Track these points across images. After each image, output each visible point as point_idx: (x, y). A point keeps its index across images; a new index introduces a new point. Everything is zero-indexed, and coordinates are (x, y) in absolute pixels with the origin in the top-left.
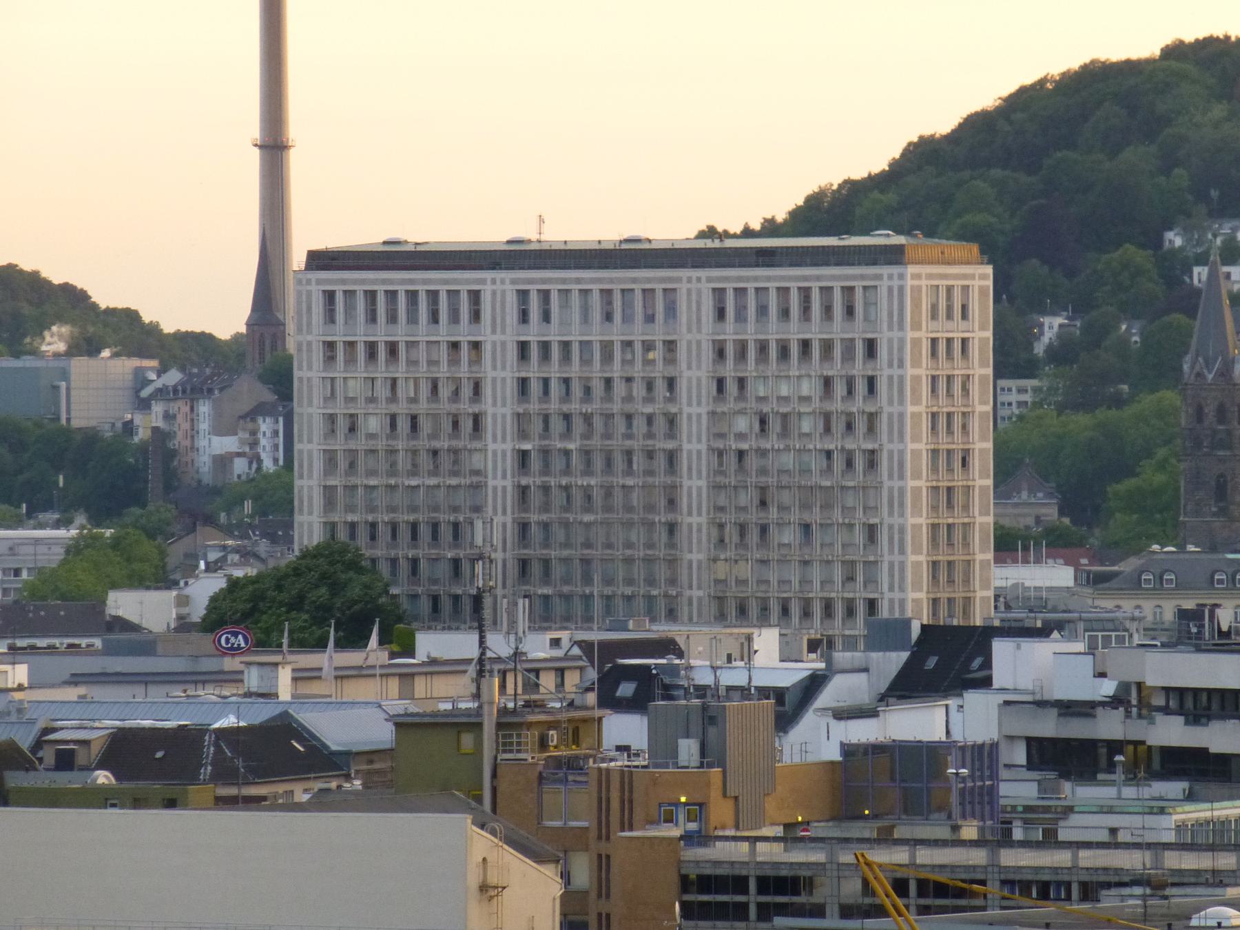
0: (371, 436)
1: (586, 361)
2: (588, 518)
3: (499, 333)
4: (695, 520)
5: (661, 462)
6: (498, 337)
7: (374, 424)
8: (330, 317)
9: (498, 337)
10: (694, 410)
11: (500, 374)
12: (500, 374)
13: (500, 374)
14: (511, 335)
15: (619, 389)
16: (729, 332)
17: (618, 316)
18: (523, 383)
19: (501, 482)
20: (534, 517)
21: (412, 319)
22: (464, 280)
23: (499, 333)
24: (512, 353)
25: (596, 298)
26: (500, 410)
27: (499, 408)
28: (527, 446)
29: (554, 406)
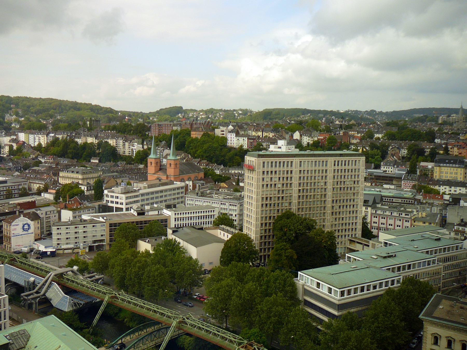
0: (279, 188)
1: (311, 173)
2: (311, 200)
3: (296, 169)
4: (329, 199)
5: (323, 190)
6: (296, 169)
7: (280, 186)
8: (264, 167)
9: (296, 169)
10: (330, 181)
11: (296, 176)
12: (296, 176)
13: (296, 176)
14: (298, 170)
15: (316, 178)
16: (336, 167)
17: (317, 165)
18: (300, 177)
19: (295, 195)
20: (301, 200)
21: (280, 166)
22: (290, 159)
23: (296, 169)
24: (298, 172)
25: (278, 163)
26: (296, 182)
27: (295, 182)
28: (300, 188)
29: (305, 181)
